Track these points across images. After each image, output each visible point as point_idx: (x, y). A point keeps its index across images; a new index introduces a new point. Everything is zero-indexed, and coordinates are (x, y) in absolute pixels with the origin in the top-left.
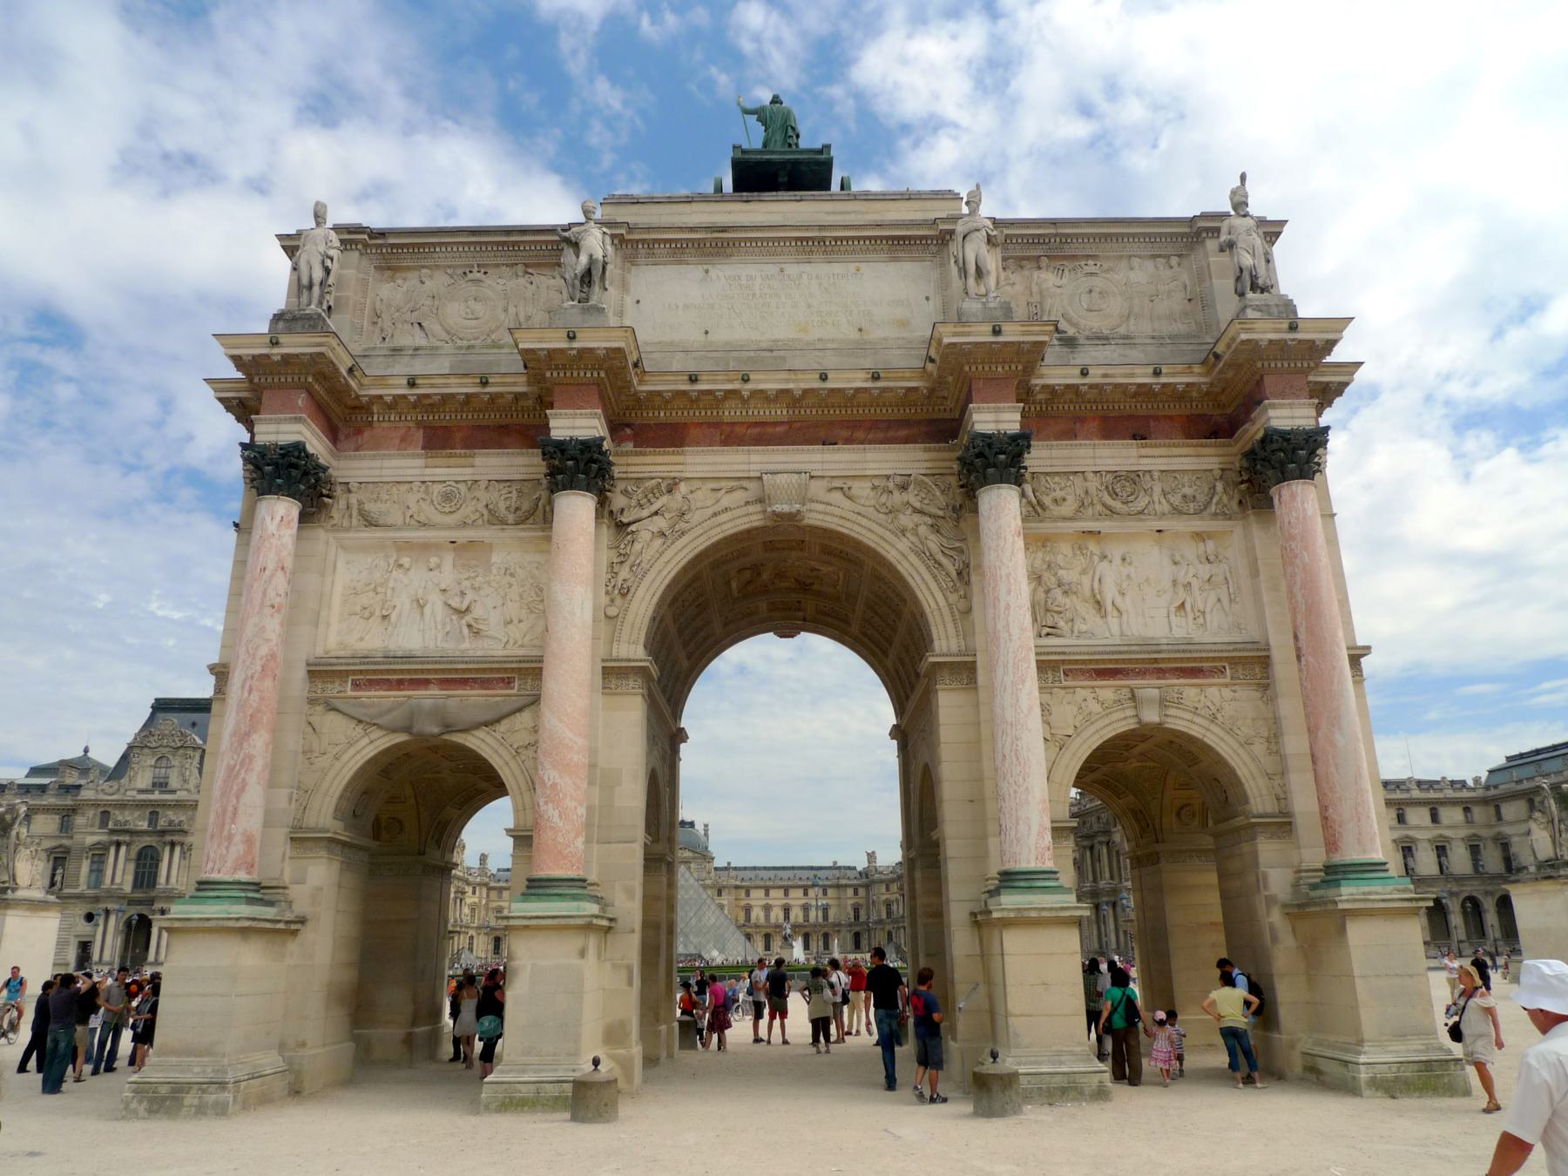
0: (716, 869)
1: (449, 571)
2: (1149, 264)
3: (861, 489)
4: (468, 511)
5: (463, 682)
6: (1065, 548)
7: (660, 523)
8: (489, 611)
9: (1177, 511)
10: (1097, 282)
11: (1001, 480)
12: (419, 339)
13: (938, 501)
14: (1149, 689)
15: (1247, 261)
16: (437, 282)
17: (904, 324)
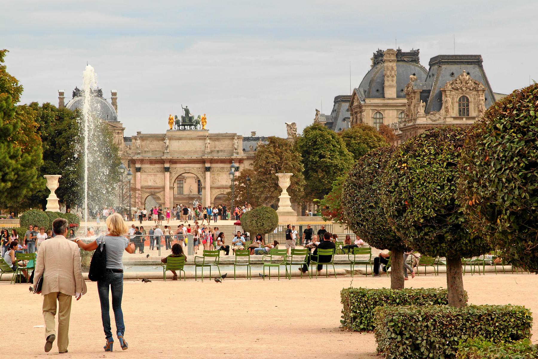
0: (126, 139)
1: (153, 177)
2: (229, 141)
3: (195, 169)
4: (155, 171)
5: (156, 189)
6: (216, 175)
7: (175, 172)
8: (158, 181)
9: (227, 172)
10: (223, 143)
11: (208, 171)
12: (147, 150)
13: (203, 170)
14: (222, 190)
15: (235, 146)
16: (148, 142)
17: (200, 148)
